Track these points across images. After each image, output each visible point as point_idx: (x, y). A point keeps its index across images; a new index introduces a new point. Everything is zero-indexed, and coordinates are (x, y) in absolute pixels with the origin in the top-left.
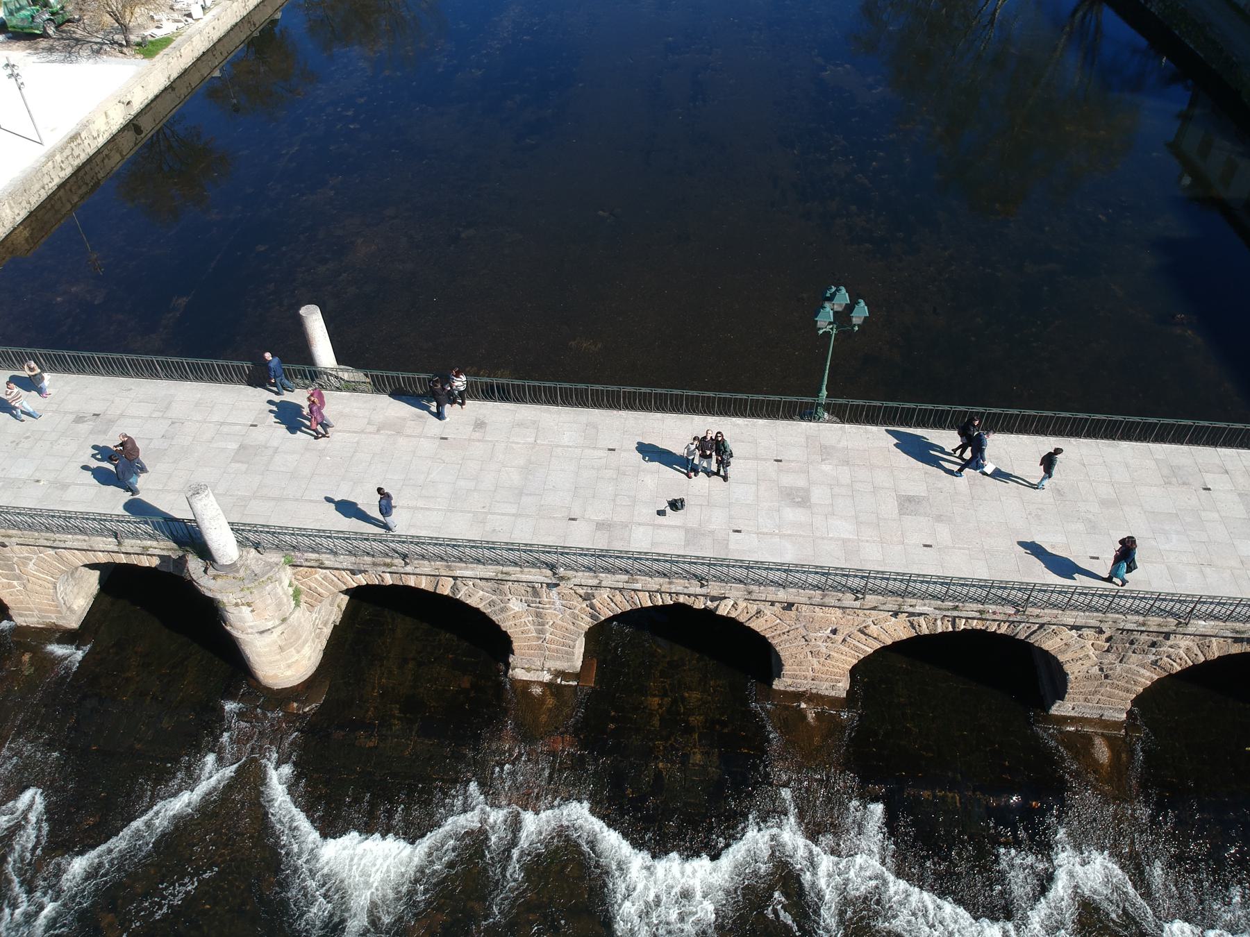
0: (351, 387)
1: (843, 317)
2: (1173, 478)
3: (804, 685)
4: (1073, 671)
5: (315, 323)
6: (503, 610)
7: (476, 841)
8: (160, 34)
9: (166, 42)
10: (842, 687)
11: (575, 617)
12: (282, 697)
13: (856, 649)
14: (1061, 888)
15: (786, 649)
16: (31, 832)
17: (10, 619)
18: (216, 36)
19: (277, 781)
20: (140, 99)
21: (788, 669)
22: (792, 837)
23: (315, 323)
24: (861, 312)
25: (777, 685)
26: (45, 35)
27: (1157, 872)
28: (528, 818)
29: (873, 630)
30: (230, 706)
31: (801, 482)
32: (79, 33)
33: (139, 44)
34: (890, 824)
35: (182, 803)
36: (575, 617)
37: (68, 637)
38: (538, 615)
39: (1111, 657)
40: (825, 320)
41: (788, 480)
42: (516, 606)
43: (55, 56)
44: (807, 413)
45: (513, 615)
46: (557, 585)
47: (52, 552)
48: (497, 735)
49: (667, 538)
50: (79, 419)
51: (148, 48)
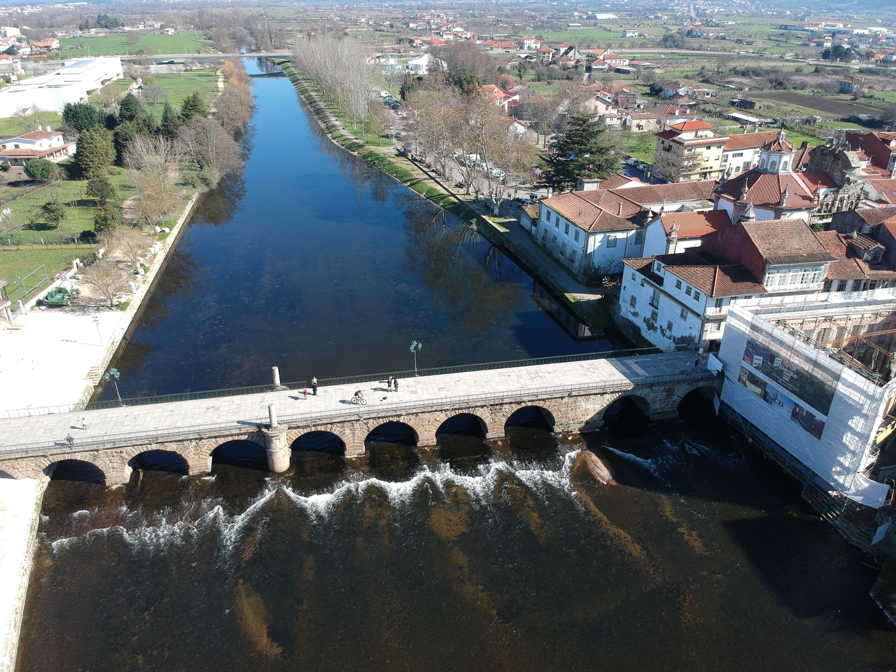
0: (283, 390)
1: (416, 348)
2: (501, 375)
3: (426, 443)
4: (486, 421)
5: (276, 370)
7: (349, 491)
8: (122, 300)
10: (435, 440)
12: (282, 474)
14: (492, 470)
15: (419, 430)
16: (222, 514)
17: (187, 474)
18: (142, 298)
19: (289, 491)
21: (420, 438)
22: (428, 473)
23: (276, 370)
24: (420, 346)
25: (419, 444)
26: (67, 305)
27: (515, 463)
28: (361, 483)
29: (438, 418)
30: (267, 479)
32: (82, 303)
33: (117, 305)
34: (451, 467)
37: (208, 474)
40: (412, 348)
42: (348, 431)
43: (78, 313)
44: (412, 375)
47: (214, 440)
48: (347, 469)
49: (385, 405)
50: (208, 409)
51: (122, 307)
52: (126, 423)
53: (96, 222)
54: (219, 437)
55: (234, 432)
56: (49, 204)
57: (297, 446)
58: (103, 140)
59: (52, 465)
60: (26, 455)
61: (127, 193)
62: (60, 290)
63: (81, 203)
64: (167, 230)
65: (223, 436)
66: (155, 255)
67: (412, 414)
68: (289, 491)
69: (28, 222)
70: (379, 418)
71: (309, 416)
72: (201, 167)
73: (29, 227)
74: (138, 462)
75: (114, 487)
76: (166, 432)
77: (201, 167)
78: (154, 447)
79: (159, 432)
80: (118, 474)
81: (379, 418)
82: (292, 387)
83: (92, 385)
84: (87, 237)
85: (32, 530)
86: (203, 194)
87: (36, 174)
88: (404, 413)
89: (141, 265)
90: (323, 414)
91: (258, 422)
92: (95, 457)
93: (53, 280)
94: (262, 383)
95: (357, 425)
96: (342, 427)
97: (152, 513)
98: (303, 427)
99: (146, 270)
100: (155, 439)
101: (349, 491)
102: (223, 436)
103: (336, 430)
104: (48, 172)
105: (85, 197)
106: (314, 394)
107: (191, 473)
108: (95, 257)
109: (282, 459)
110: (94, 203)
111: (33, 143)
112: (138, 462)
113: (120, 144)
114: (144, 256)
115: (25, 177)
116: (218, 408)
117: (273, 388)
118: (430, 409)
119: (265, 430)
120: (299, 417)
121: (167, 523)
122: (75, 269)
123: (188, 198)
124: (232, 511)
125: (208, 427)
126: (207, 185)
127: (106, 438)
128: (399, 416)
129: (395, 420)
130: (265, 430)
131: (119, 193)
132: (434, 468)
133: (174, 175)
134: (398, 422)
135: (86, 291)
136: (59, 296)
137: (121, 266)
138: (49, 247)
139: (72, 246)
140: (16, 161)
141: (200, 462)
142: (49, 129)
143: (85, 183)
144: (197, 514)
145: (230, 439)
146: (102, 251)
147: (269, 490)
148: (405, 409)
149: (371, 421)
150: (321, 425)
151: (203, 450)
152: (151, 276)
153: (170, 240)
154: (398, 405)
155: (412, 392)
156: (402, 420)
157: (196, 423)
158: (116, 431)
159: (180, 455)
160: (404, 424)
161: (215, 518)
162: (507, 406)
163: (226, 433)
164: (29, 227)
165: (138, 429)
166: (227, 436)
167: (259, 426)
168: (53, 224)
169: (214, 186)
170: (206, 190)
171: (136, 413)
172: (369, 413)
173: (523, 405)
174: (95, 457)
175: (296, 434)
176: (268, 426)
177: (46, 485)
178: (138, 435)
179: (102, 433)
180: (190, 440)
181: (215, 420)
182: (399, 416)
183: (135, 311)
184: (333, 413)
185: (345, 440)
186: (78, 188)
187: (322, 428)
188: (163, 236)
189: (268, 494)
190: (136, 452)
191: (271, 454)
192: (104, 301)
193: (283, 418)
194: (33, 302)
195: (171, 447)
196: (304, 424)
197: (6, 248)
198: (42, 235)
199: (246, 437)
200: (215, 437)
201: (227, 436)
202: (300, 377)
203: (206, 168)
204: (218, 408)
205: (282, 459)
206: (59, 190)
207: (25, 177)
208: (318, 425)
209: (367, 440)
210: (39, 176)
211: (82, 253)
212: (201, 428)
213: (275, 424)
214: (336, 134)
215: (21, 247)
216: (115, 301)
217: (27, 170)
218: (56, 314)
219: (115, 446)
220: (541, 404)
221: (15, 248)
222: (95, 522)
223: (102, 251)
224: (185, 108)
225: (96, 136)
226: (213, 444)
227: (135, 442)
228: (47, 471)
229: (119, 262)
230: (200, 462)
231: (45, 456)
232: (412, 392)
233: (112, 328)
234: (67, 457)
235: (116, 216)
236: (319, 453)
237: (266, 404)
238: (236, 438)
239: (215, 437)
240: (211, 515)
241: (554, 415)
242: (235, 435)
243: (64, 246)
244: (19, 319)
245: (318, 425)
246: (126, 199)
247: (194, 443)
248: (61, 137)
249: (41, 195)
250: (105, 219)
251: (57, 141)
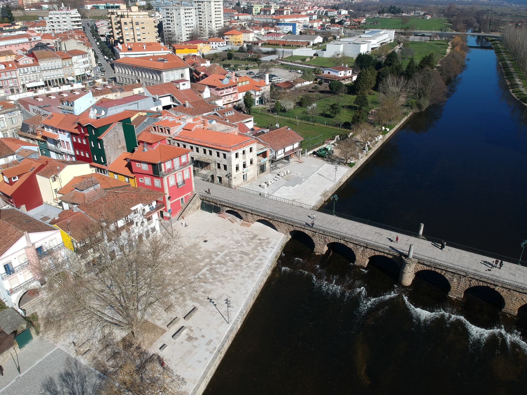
0: (422, 239)
3: (509, 311)
6: (452, 281)
7: (443, 316)
8: (352, 162)
9: (354, 164)
10: (517, 312)
11: (466, 285)
13: (520, 303)
15: (507, 301)
19: (406, 298)
20: (349, 175)
22: (503, 332)
25: (503, 310)
31: (514, 273)
32: (333, 158)
35: (388, 297)
36: (466, 285)
37: (364, 268)
38: (459, 283)
41: (511, 272)
42: (455, 280)
44: (516, 262)
45: (454, 282)
46: (465, 276)
49: (488, 274)
51: (351, 165)
52: (333, 224)
53: (353, 118)
54: (377, 251)
55: (386, 251)
56: (334, 105)
57: (419, 275)
58: (371, 75)
59: (294, 231)
60: (285, 222)
61: (374, 106)
62: (325, 149)
63: (350, 107)
64: (388, 129)
65: (379, 251)
66: (377, 142)
67: (506, 288)
68: (406, 298)
69: (322, 112)
70: (481, 281)
71: (433, 260)
72: (419, 98)
73: (322, 115)
74: (332, 246)
75: (317, 254)
76: (350, 236)
77: (419, 98)
78: (342, 242)
79: (347, 235)
80: (321, 249)
81: (481, 281)
82: (428, 239)
83: (324, 200)
84: (347, 125)
85: (276, 257)
86: (415, 114)
87: (334, 87)
88: (500, 285)
89: (368, 146)
90: (442, 263)
91: (401, 251)
92: (314, 235)
93: (323, 143)
94: (413, 232)
95: (463, 279)
96: (453, 276)
97: (330, 275)
98: (427, 266)
99: (370, 149)
100: (344, 238)
101: (443, 316)
102: (379, 251)
103: (448, 276)
104: (339, 88)
105: (352, 104)
106: (441, 249)
107: (355, 264)
108: (347, 136)
109: (408, 279)
110: (356, 108)
111: (337, 72)
112: (332, 246)
113: (379, 79)
114: (371, 141)
115: (328, 89)
116: (382, 235)
117: (416, 235)
118: (521, 290)
119: (403, 258)
120: (427, 258)
121: (335, 283)
122: (335, 141)
123: (406, 114)
124: (371, 293)
125: (372, 243)
126: (420, 108)
127: (321, 228)
128: (496, 286)
129: (492, 287)
130: (403, 258)
131: (370, 105)
132: (509, 330)
133: (402, 100)
134: (493, 289)
135: (337, 153)
136: (324, 152)
137: (358, 144)
138: (327, 126)
139: (338, 128)
140: (326, 81)
141: (363, 260)
142: (347, 66)
143: (355, 97)
144: (351, 287)
145: (382, 254)
146: (351, 134)
147: (395, 293)
148: (502, 283)
149: (474, 281)
150: (439, 269)
152: (371, 153)
153: (388, 136)
154: (497, 279)
155: (512, 274)
156: (497, 289)
157: (369, 237)
158: (327, 226)
159: (353, 252)
160: (497, 292)
161: (361, 292)
163: (381, 250)
164: (322, 115)
165: (337, 229)
166: (381, 252)
167: (401, 254)
168: (333, 115)
169: (424, 109)
170: (418, 111)
171: (339, 221)
172: (474, 275)
174: (314, 235)
175: (421, 268)
176: (407, 256)
177: (289, 239)
178: (337, 232)
179: (320, 225)
180: (361, 246)
181: (378, 240)
182: (496, 286)
183: (356, 169)
184: (449, 265)
185: (452, 285)
186: (351, 99)
187: (439, 271)
188: (385, 132)
189: (393, 295)
190: (333, 240)
191: (403, 273)
192: (343, 160)
193: (417, 255)
194: (311, 152)
195: (350, 246)
196: (428, 264)
197: (309, 123)
198: (326, 120)
199: (392, 257)
200: (375, 250)
201: (381, 252)
202: (437, 236)
203: (422, 99)
204: (382, 235)
205: (408, 279)
206: (342, 99)
207: (328, 89)
208: (437, 268)
209: (467, 292)
210: (334, 90)
211: (341, 133)
212: (369, 242)
213: (411, 256)
214: (517, 89)
215: (315, 124)
216: (349, 161)
217: (330, 86)
218: (320, 161)
219: (324, 234)
221: (312, 124)
222: (303, 267)
223: (351, 134)
224: (422, 62)
225: (369, 73)
226: (372, 253)
227: (333, 236)
228: (292, 233)
229: (357, 141)
230: (363, 260)
231: (293, 226)
232: (512, 274)
233: (342, 174)
234: (302, 230)
235: (364, 117)
236: (432, 285)
237: (410, 243)
238: (386, 255)
239: (375, 250)
240: (358, 290)
242: (386, 253)
243: (334, 128)
244: (303, 158)
245: (437, 268)
246: (372, 109)
247: (362, 249)
248: (351, 71)
249: (333, 100)
250: (358, 117)
251: (349, 73)
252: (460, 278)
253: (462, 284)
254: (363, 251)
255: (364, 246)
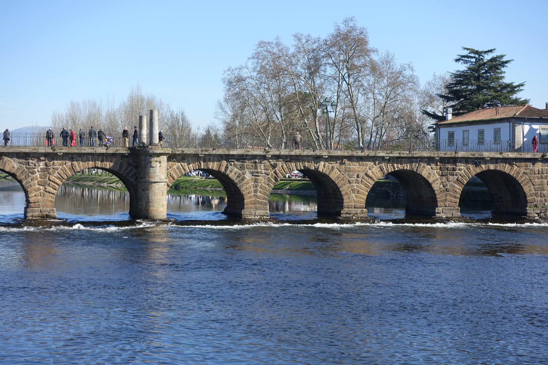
4: (436, 186)
6: (243, 179)
11: (269, 180)
15: (344, 189)
39: (444, 178)
42: (248, 176)
95: (261, 168)
96: (242, 168)
151: (52, 178)
162: (462, 166)
173: (484, 167)
185: (244, 190)
220: (506, 168)
241: (526, 189)
247: (42, 164)
252: (256, 168)
253: (262, 179)
254: (46, 169)
255: (46, 155)
